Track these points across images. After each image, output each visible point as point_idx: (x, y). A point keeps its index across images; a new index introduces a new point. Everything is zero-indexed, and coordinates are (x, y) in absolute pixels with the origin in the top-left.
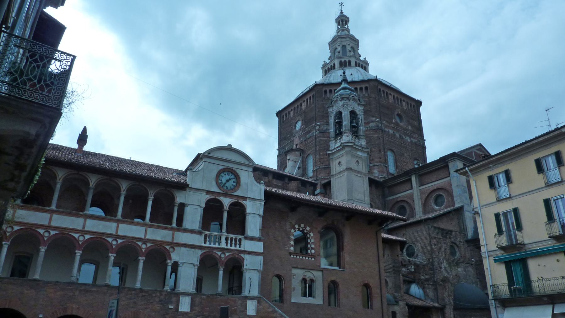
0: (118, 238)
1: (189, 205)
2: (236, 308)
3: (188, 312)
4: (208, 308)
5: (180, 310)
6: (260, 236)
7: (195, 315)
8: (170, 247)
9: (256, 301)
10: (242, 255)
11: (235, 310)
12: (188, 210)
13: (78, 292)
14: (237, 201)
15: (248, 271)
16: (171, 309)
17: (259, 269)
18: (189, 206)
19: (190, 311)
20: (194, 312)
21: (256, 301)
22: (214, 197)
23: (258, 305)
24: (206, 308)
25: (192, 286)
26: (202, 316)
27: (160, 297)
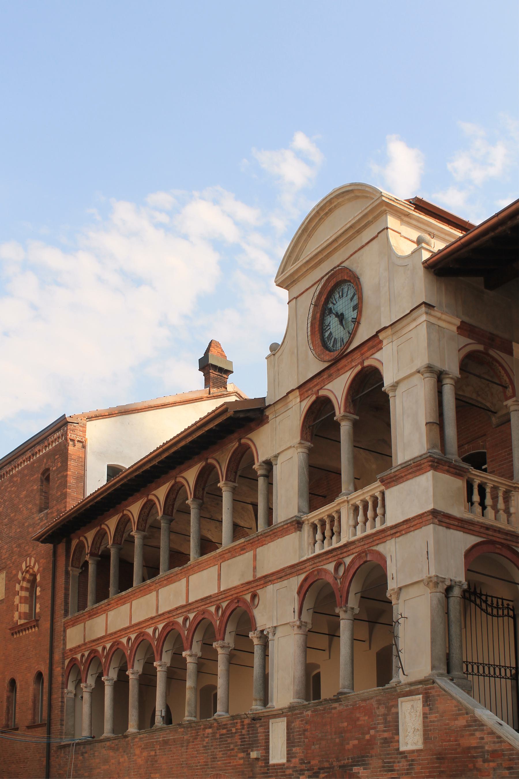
0: (189, 611)
1: (276, 457)
2: (372, 732)
3: (283, 764)
4: (317, 746)
5: (272, 761)
6: (428, 449)
7: (297, 771)
8: (250, 594)
9: (421, 696)
10: (380, 548)
11: (371, 743)
12: (277, 470)
13: (158, 747)
14: (359, 367)
15: (404, 595)
16: (257, 759)
17: (424, 576)
18: (280, 460)
19: (287, 762)
20: (293, 760)
21: (421, 696)
22: (314, 398)
23: (427, 708)
24: (313, 747)
25: (292, 688)
26: (308, 770)
27: (241, 732)
